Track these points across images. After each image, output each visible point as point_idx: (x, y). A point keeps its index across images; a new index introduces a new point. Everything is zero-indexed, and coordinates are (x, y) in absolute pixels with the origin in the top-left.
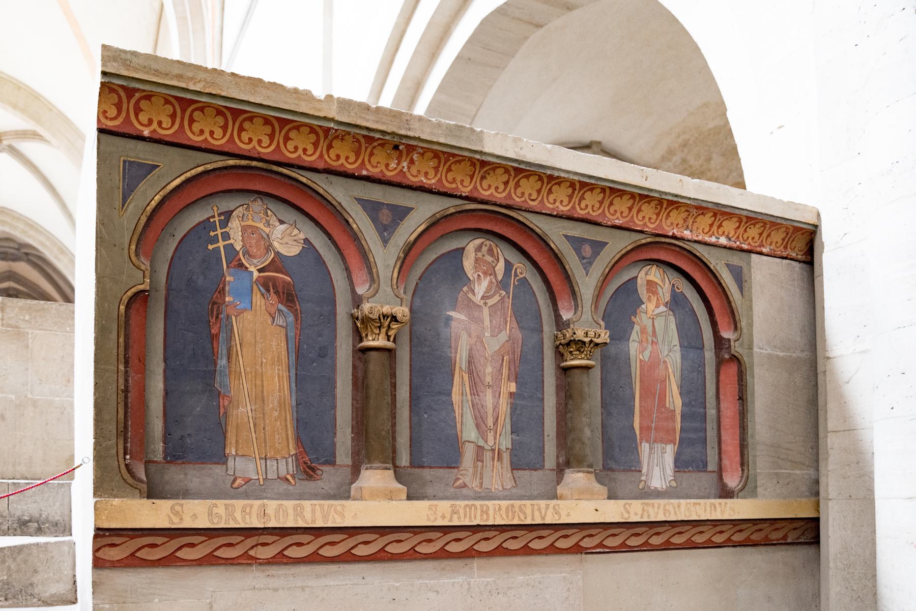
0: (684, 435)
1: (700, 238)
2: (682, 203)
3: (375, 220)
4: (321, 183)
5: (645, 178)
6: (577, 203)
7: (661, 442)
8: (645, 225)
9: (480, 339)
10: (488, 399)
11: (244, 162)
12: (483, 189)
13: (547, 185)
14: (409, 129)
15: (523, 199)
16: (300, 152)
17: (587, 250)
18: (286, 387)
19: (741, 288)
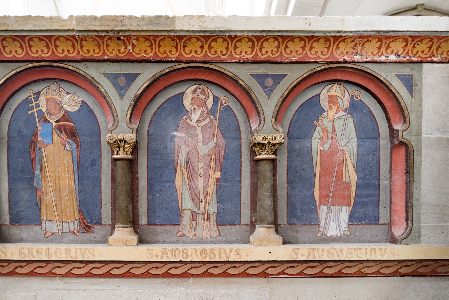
0: (358, 200)
1: (370, 59)
2: (345, 36)
3: (115, 84)
4: (82, 68)
5: (308, 24)
6: (258, 51)
7: (338, 205)
8: (318, 57)
9: (195, 147)
10: (201, 183)
11: (37, 64)
12: (186, 54)
13: (232, 43)
14: (123, 26)
15: (216, 56)
16: (66, 52)
17: (269, 82)
18: (72, 183)
19: (411, 92)
